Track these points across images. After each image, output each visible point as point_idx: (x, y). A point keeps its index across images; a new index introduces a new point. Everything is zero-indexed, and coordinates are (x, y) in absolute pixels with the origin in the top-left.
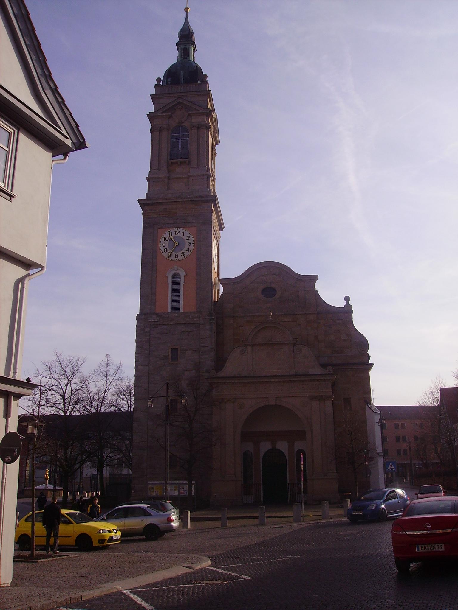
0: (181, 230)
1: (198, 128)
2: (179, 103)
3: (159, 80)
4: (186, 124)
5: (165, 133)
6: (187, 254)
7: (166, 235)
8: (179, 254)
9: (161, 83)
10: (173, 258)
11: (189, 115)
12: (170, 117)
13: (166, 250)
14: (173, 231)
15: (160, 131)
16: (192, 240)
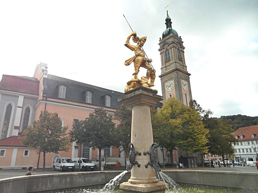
0: (170, 81)
1: (171, 48)
2: (165, 43)
3: (160, 38)
4: (168, 49)
5: (163, 54)
6: (172, 88)
7: (167, 84)
8: (171, 89)
9: (162, 39)
10: (169, 91)
11: (168, 45)
12: (164, 48)
13: (167, 89)
14: (168, 82)
15: (162, 53)
16: (173, 84)
